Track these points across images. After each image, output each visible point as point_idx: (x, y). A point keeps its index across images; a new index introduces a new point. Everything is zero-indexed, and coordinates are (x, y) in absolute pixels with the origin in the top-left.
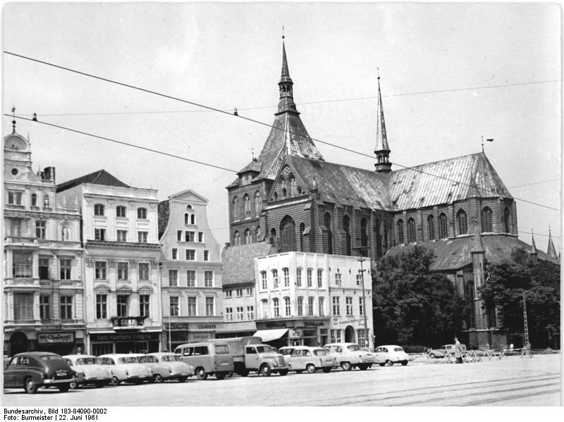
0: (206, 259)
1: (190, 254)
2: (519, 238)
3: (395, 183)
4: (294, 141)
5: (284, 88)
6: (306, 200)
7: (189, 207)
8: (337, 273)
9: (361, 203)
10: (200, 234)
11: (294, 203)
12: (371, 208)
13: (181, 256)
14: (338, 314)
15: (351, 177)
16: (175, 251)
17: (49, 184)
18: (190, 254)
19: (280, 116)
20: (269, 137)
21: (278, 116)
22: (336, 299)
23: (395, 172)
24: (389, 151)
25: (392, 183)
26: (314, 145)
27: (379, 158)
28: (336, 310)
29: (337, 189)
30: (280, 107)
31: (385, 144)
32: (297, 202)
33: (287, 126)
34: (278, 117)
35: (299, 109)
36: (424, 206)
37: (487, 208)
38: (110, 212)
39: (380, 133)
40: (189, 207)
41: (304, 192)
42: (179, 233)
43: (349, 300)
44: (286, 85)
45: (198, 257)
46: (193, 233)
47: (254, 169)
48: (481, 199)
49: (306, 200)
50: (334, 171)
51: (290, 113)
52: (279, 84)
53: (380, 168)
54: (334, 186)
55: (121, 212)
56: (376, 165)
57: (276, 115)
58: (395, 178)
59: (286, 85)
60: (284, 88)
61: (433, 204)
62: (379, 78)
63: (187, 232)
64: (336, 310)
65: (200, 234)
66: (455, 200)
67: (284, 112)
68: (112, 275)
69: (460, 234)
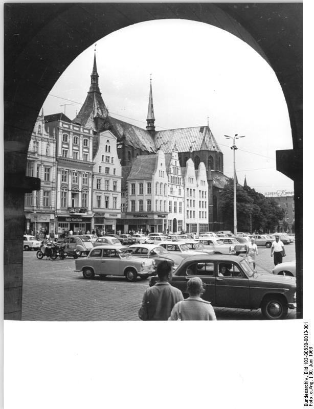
1: (107, 169)
3: (158, 138)
7: (108, 141)
10: (112, 158)
13: (103, 171)
15: (137, 132)
16: (100, 167)
18: (107, 169)
23: (158, 132)
28: (170, 210)
40: (108, 141)
45: (111, 172)
46: (109, 157)
48: (208, 151)
53: (150, 129)
55: (76, 140)
58: (158, 135)
64: (170, 210)
65: (112, 158)
66: (194, 150)
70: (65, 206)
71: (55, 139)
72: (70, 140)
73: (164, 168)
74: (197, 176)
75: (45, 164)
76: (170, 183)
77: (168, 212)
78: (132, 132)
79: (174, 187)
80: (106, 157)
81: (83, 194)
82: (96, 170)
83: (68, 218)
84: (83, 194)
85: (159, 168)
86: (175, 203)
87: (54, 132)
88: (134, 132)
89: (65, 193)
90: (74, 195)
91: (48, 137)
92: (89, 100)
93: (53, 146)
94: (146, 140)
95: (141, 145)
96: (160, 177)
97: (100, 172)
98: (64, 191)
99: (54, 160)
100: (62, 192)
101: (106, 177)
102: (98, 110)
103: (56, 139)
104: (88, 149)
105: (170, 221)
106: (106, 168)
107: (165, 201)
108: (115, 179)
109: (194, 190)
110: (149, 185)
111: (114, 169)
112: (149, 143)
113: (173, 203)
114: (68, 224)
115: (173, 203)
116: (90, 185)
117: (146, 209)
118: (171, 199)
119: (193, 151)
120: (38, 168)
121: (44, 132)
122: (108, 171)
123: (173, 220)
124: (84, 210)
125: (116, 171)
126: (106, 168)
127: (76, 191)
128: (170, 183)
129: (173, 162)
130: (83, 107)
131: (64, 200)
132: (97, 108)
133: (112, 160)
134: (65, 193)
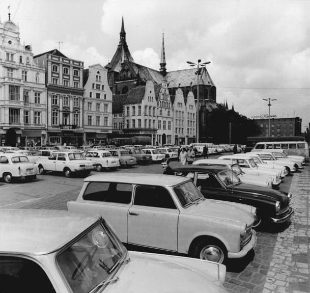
1: (98, 95)
7: (98, 72)
13: (94, 96)
16: (91, 93)
18: (98, 95)
22: (160, 122)
28: (159, 127)
38: (60, 70)
40: (98, 72)
42: (93, 84)
45: (102, 97)
46: (99, 85)
55: (65, 71)
64: (159, 127)
65: (103, 86)
70: (56, 123)
72: (60, 70)
75: (35, 89)
79: (163, 110)
80: (97, 85)
82: (87, 95)
84: (75, 115)
85: (147, 94)
86: (165, 122)
99: (44, 87)
105: (160, 135)
107: (154, 121)
108: (106, 103)
113: (162, 122)
115: (162, 122)
116: (81, 107)
124: (74, 126)
125: (107, 96)
134: (57, 114)
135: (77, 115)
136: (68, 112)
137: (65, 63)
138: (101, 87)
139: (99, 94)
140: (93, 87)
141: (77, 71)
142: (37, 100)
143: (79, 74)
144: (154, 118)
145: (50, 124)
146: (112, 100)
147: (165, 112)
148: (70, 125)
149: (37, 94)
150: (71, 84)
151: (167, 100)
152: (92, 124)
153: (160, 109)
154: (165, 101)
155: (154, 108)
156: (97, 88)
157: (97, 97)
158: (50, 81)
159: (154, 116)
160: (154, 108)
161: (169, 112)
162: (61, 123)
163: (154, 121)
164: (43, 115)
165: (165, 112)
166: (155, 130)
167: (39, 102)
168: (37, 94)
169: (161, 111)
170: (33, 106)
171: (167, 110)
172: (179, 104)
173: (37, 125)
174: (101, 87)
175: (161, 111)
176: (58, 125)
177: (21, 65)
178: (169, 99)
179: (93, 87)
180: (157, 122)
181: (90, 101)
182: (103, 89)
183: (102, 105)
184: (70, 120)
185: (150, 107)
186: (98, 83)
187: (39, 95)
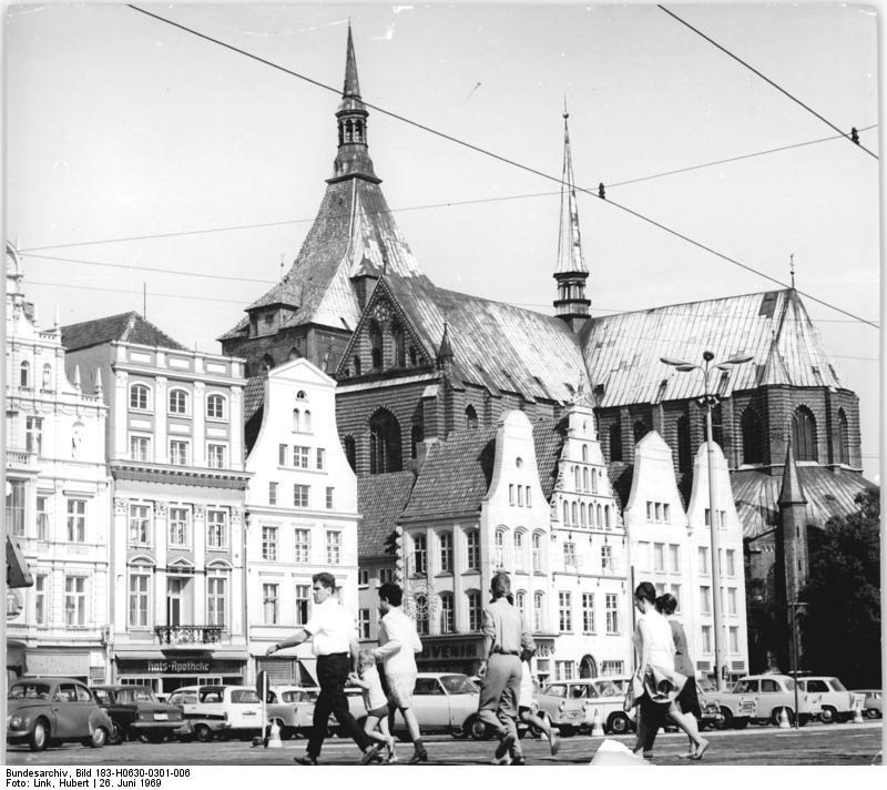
0: (329, 505)
1: (301, 495)
2: (864, 475)
3: (599, 346)
4: (370, 241)
5: (349, 124)
6: (427, 377)
7: (301, 395)
8: (568, 541)
9: (535, 386)
10: (320, 451)
11: (399, 381)
12: (555, 397)
13: (286, 498)
14: (569, 628)
15: (510, 328)
16: (273, 485)
17: (51, 340)
18: (301, 495)
19: (340, 185)
20: (313, 231)
21: (334, 186)
22: (564, 597)
23: (600, 320)
24: (585, 275)
25: (594, 344)
26: (409, 251)
27: (566, 285)
28: (565, 625)
29: (486, 355)
30: (338, 165)
31: (578, 259)
32: (408, 380)
33: (357, 207)
34: (333, 188)
35: (378, 173)
36: (667, 398)
37: (803, 409)
38: (159, 396)
39: (566, 234)
40: (301, 395)
41: (421, 360)
42: (283, 447)
43: (587, 599)
44: (352, 121)
45: (316, 500)
46: (305, 449)
47: (285, 300)
48: (792, 388)
49: (427, 377)
50: (477, 313)
51: (354, 179)
52: (338, 115)
53: (569, 310)
54: (480, 349)
55: (177, 402)
56: (556, 304)
57: (330, 182)
58: (598, 334)
59: (352, 121)
60: (349, 124)
61: (687, 396)
62: (566, 117)
63: (296, 448)
64: (565, 625)
65: (320, 451)
66: (737, 389)
67: (351, 177)
68: (160, 528)
69: (746, 462)
70: (144, 622)
71: (100, 403)
72: (159, 396)
73: (530, 475)
74: (686, 489)
75: (68, 486)
76: (560, 525)
77: (557, 630)
78: (488, 330)
79: (580, 540)
80: (296, 448)
81: (211, 580)
82: (257, 495)
83: (156, 661)
84: (211, 580)
85: (506, 472)
86: (587, 599)
87: (99, 382)
88: (495, 326)
89: (144, 578)
90: (177, 584)
91: (78, 400)
92: (336, 209)
93: (95, 427)
94: (549, 356)
95: (524, 377)
96: (513, 502)
97: (272, 501)
98: (141, 571)
99: (101, 474)
100: (133, 578)
101: (296, 520)
102: (368, 246)
103: (106, 401)
104: (226, 425)
105: (568, 663)
106: (297, 487)
107: (539, 594)
108: (334, 525)
109: (674, 547)
110: (474, 536)
111: (329, 490)
112: (562, 366)
113: (576, 601)
114: (155, 681)
115: (576, 601)
116: (237, 549)
117: (464, 625)
118: (565, 584)
119: (734, 393)
120: (41, 503)
121: (65, 385)
122: (305, 497)
123: (578, 660)
124: (212, 632)
125: (334, 494)
126: (297, 487)
127: (186, 571)
128: (560, 525)
129: (573, 450)
130: (309, 238)
131: (139, 605)
132: (365, 240)
133: (319, 460)
134: (144, 578)
135: (221, 581)
136: (186, 571)
137: (178, 370)
138: (312, 457)
139: (306, 488)
140: (282, 460)
141: (220, 399)
142: (77, 529)
143: (225, 411)
144: (539, 584)
145: (121, 623)
146: (355, 510)
147: (588, 552)
148: (191, 628)
149: (77, 504)
150: (198, 459)
151: (595, 495)
152: (281, 621)
153: (563, 537)
154: (587, 500)
155: (536, 535)
156: (297, 464)
157: (297, 503)
158: (436, 629)
159: (538, 574)
160: (536, 535)
161: (605, 550)
162: (163, 623)
163: (539, 594)
164: (96, 589)
165: (588, 552)
166: (545, 642)
167: (82, 537)
168: (77, 504)
169: (569, 547)
170: (61, 553)
171: (599, 541)
172: (657, 508)
173: (76, 629)
174: (312, 457)
175: (569, 547)
176: (150, 626)
177: (25, 395)
178: (604, 486)
179: (282, 460)
180: (552, 606)
181: (271, 521)
182: (319, 466)
183: (318, 538)
184: (196, 610)
185: (518, 534)
186: (302, 441)
187: (82, 506)
